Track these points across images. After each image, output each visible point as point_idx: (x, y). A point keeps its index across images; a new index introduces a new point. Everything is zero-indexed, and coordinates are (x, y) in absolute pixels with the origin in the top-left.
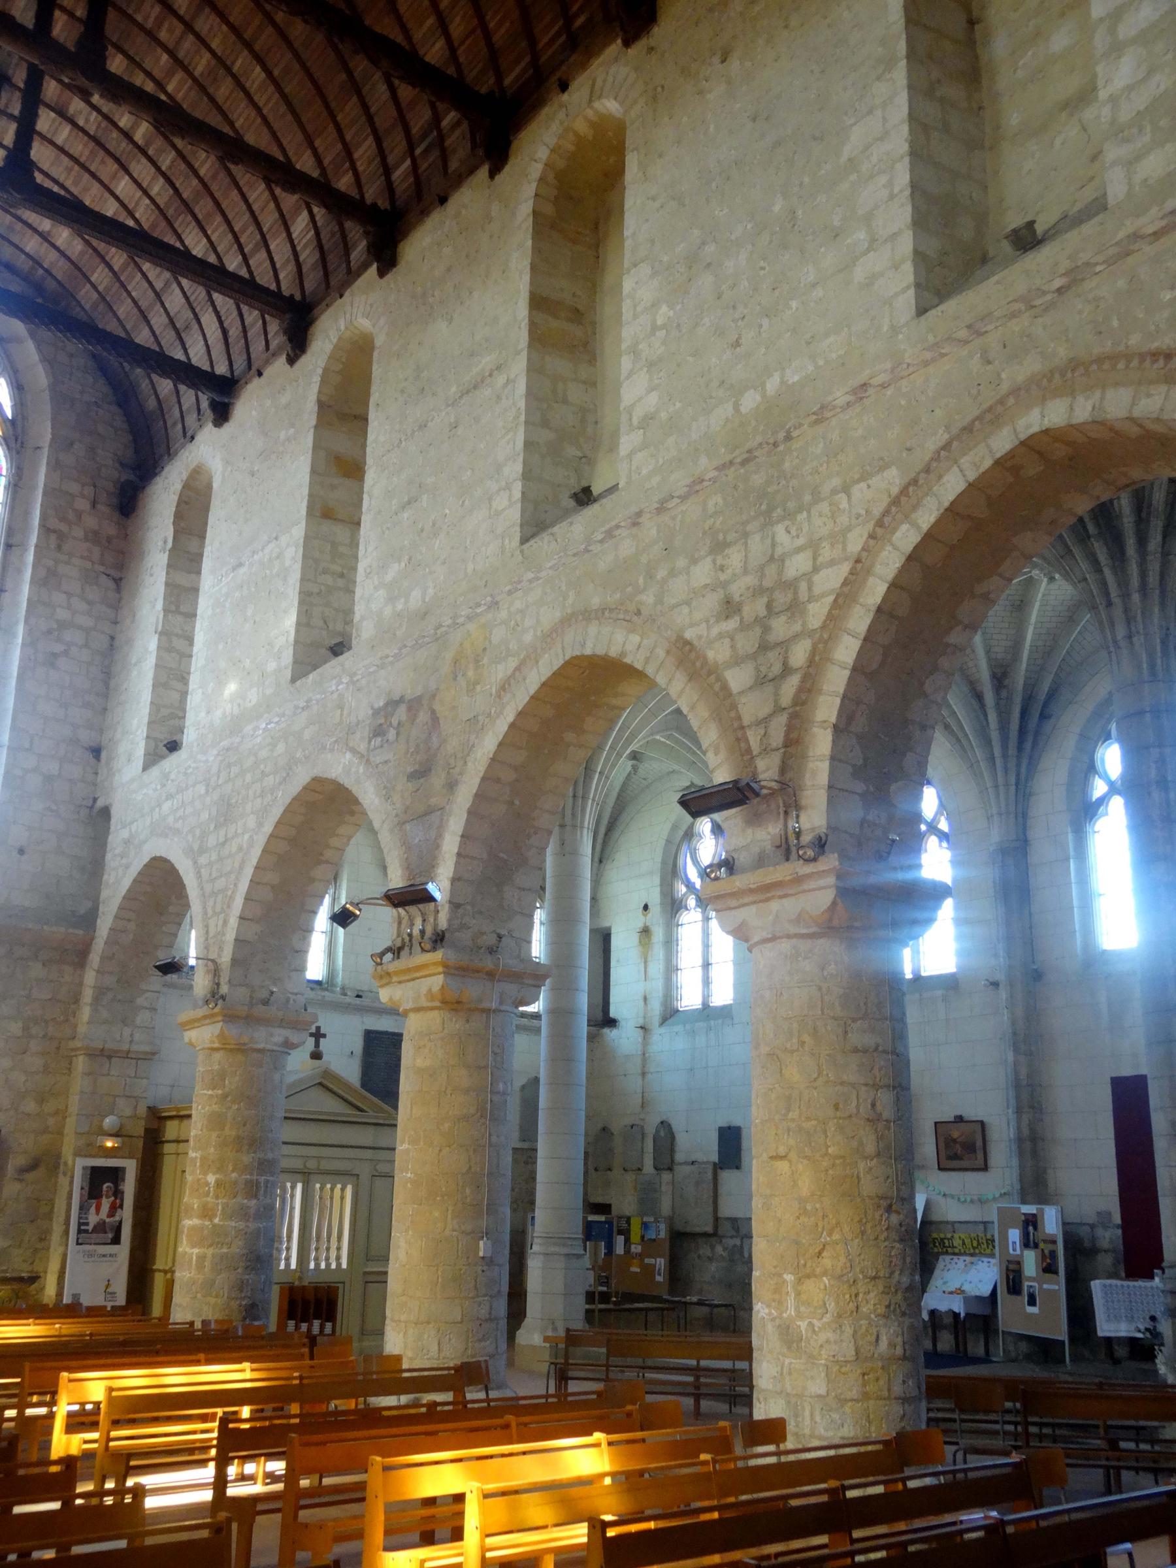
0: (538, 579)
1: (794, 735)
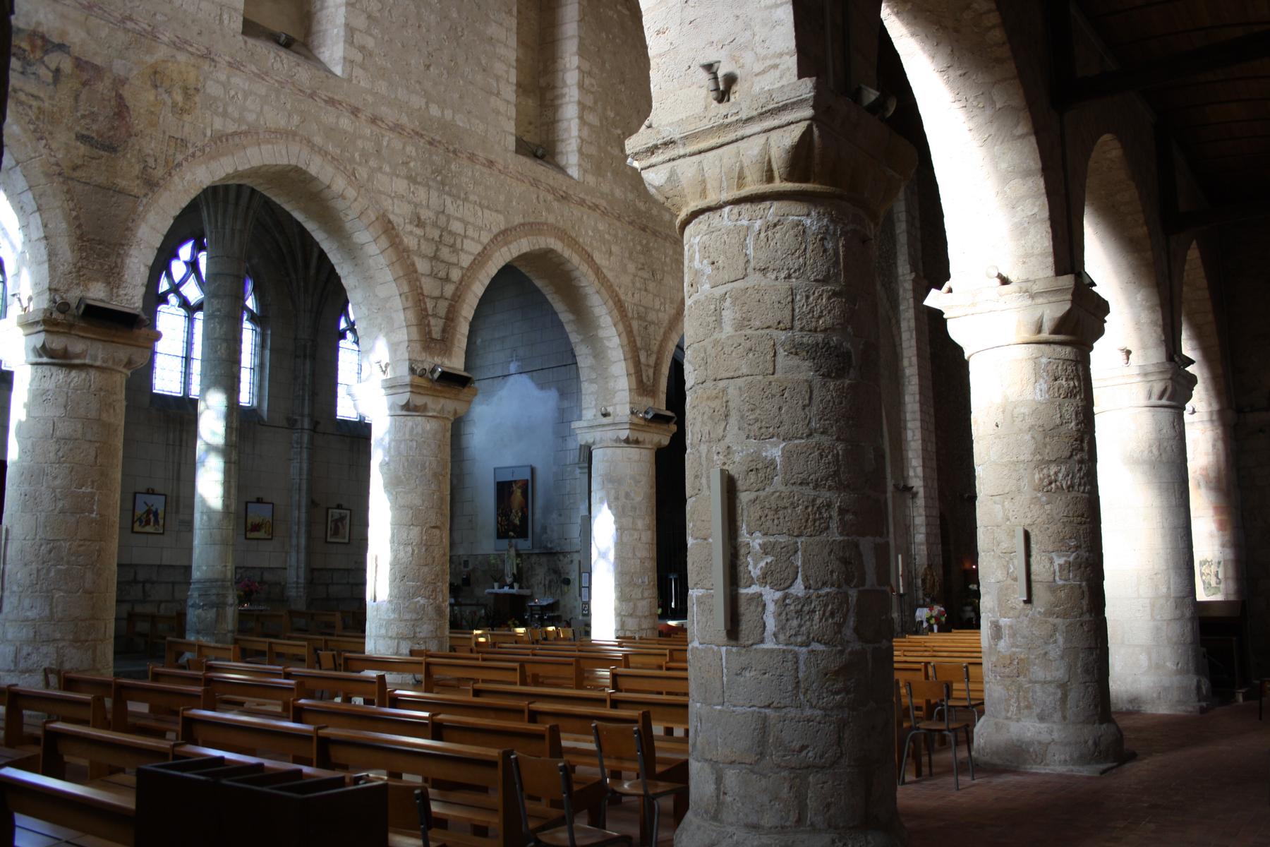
0: (263, 79)
1: (451, 316)
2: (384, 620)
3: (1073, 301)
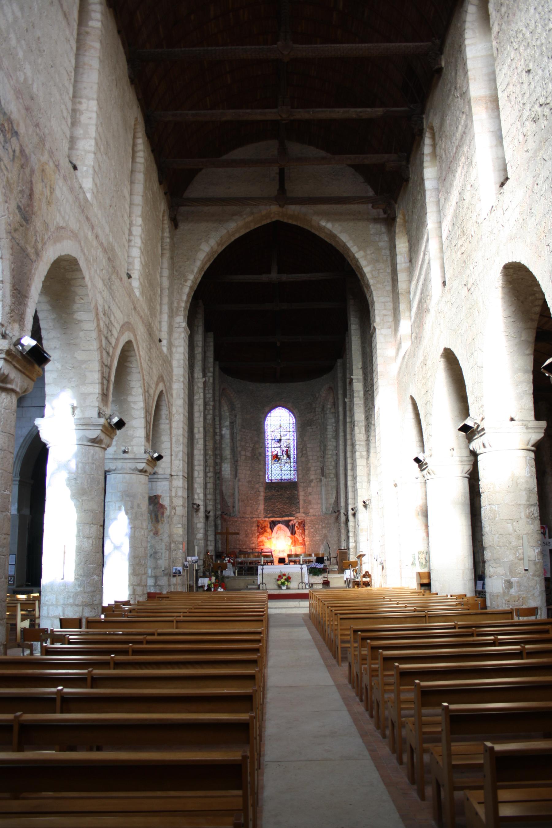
2: (72, 592)
3: (545, 433)
